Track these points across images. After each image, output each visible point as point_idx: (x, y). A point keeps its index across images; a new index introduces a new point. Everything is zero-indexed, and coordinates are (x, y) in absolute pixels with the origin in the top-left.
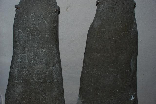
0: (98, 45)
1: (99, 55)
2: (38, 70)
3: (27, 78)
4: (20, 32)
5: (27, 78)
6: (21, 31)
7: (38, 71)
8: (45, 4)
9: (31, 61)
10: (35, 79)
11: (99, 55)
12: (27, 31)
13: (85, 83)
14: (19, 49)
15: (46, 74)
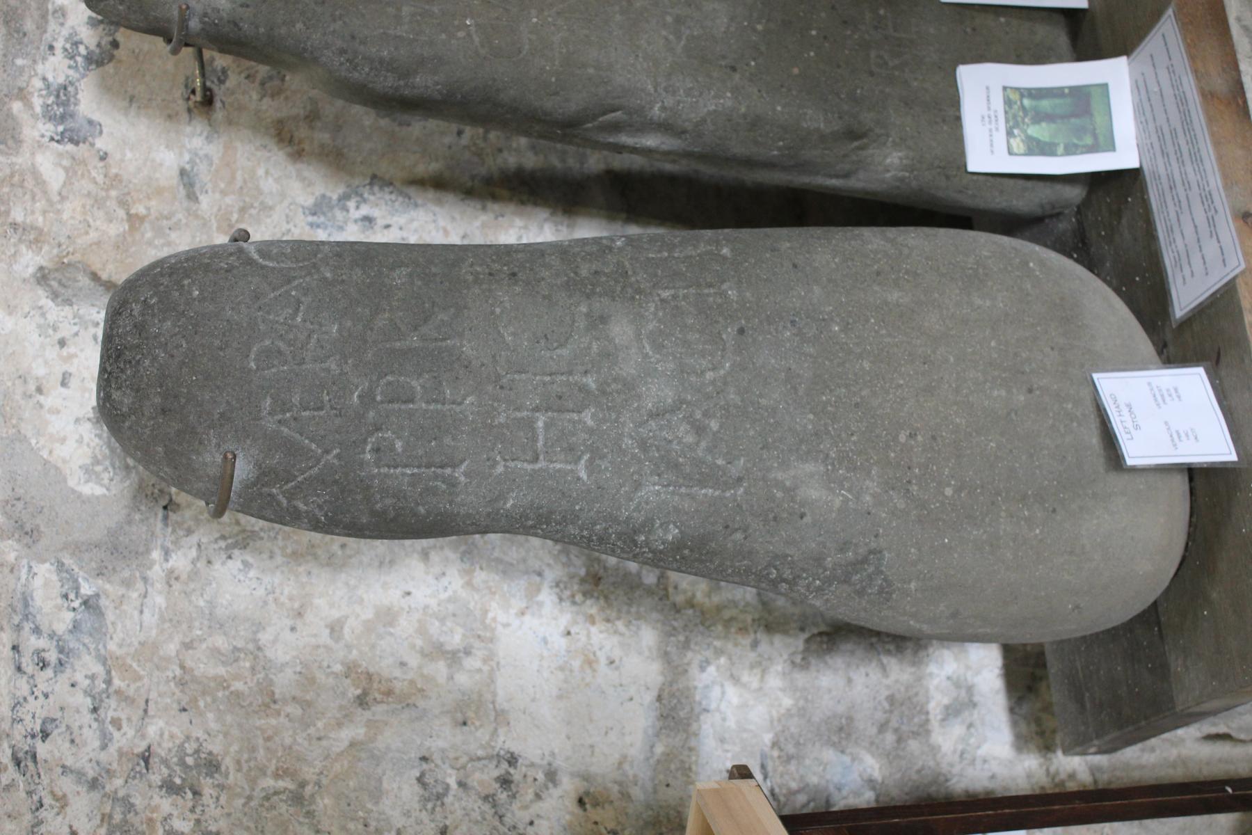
0: (466, 17)
1: (534, 12)
2: (648, 349)
3: (714, 425)
4: (377, 450)
5: (714, 425)
6: (368, 448)
7: (658, 347)
8: (186, 282)
9: (583, 389)
10: (722, 372)
11: (534, 12)
12: (368, 398)
13: (743, 110)
14: (500, 469)
15: (675, 297)
